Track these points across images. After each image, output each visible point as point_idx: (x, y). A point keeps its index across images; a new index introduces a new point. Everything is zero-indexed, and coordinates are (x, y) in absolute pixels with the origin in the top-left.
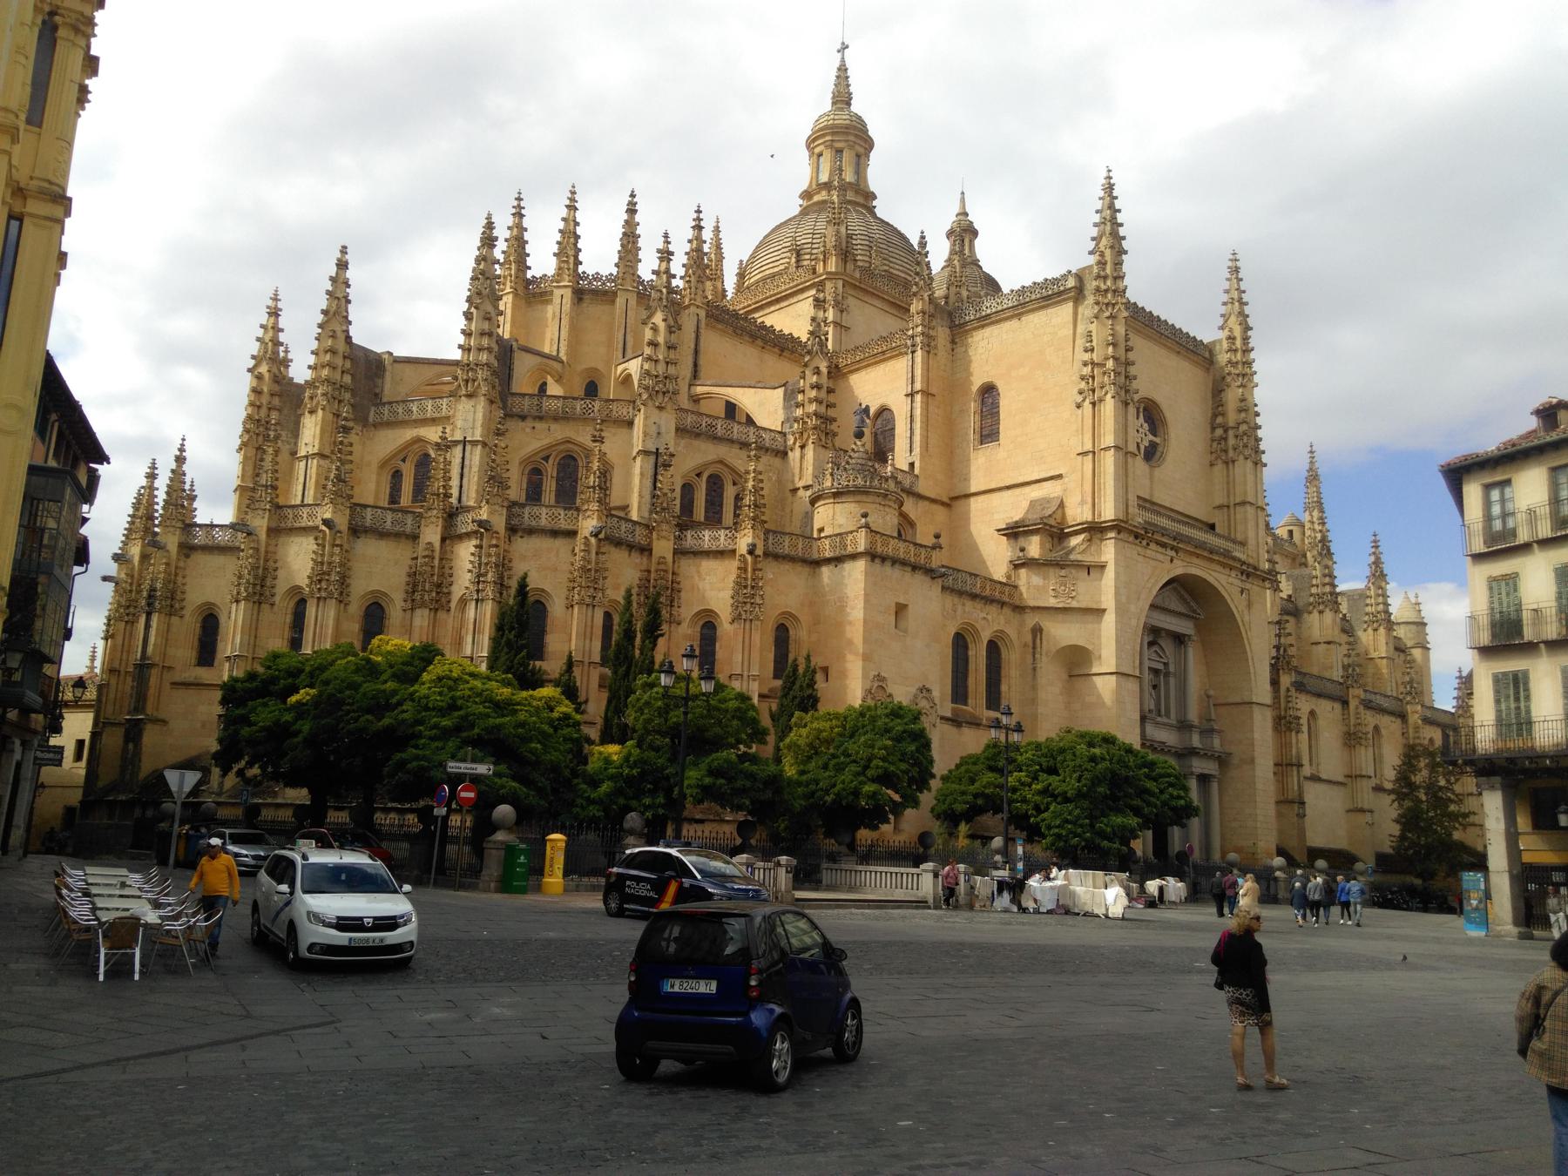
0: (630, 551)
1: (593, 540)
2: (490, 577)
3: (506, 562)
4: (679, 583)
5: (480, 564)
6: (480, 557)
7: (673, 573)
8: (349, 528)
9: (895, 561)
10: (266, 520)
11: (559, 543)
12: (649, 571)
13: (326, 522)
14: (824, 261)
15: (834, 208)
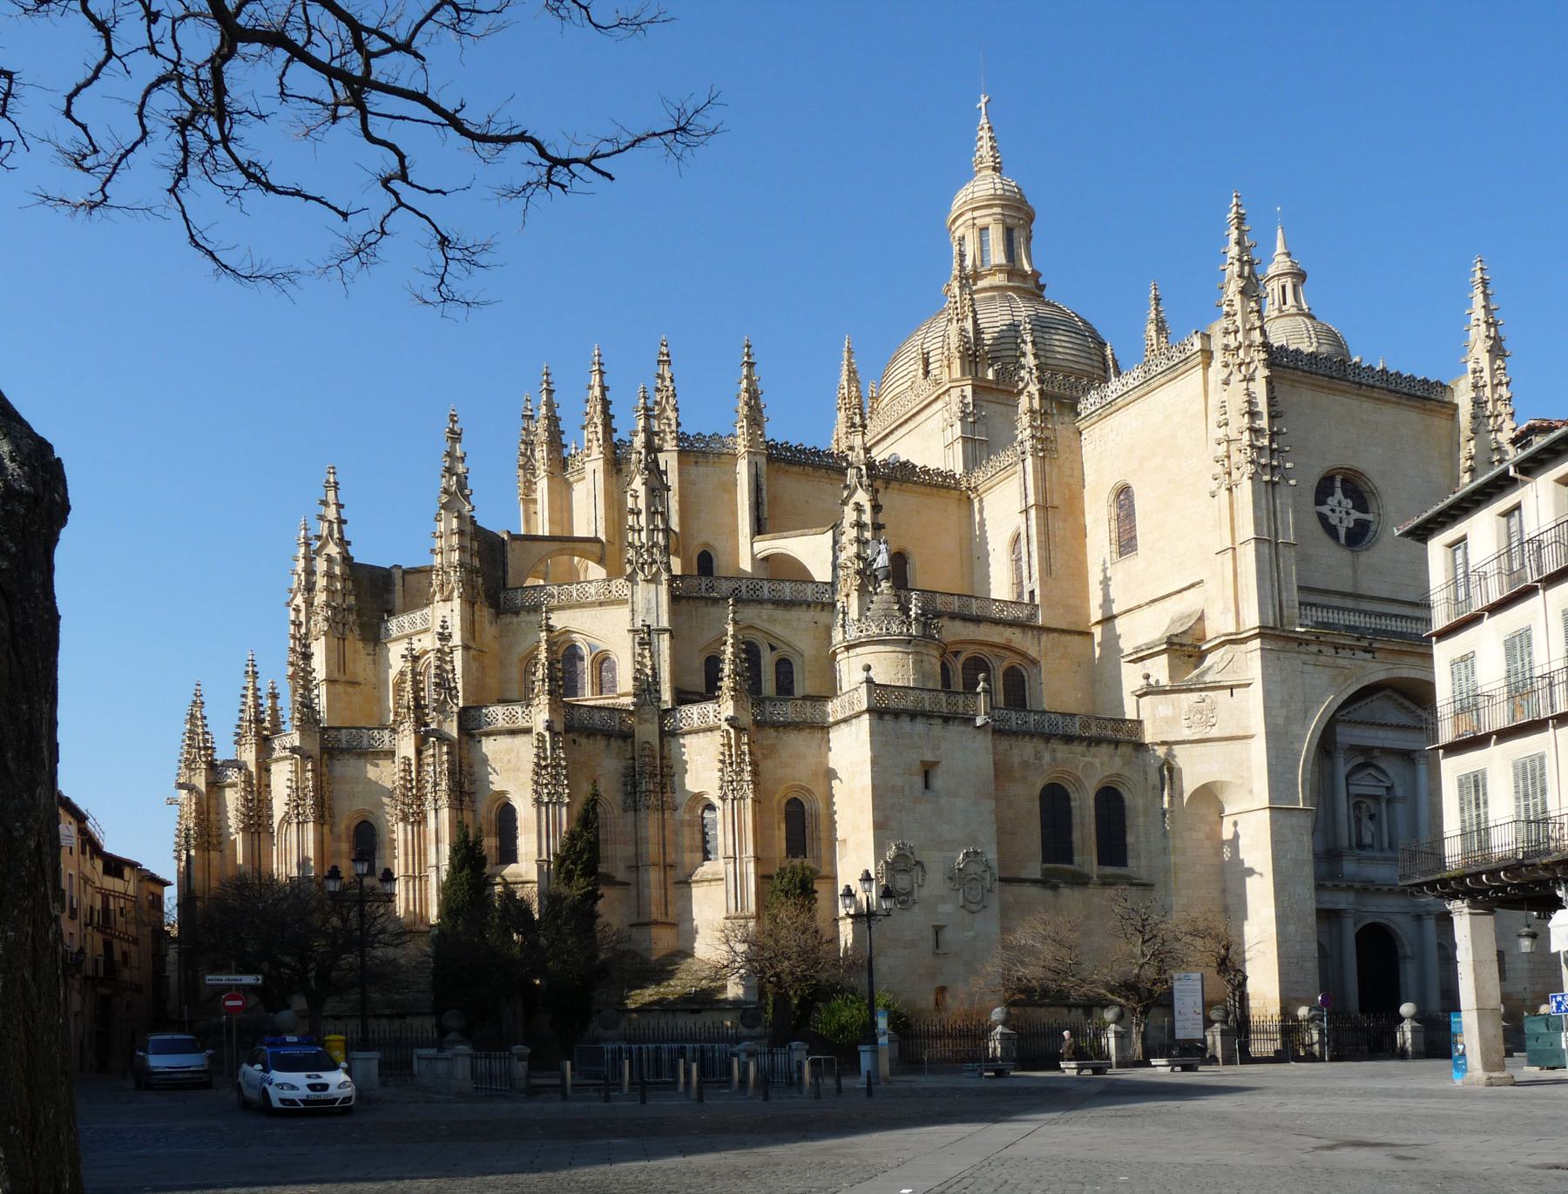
0: (609, 740)
1: (547, 734)
2: (444, 785)
3: (465, 768)
4: (672, 768)
5: (435, 773)
6: (435, 767)
7: (662, 758)
8: (322, 754)
9: (913, 715)
10: (254, 753)
11: (520, 741)
12: (633, 758)
13: (293, 750)
14: (949, 367)
15: (956, 302)
